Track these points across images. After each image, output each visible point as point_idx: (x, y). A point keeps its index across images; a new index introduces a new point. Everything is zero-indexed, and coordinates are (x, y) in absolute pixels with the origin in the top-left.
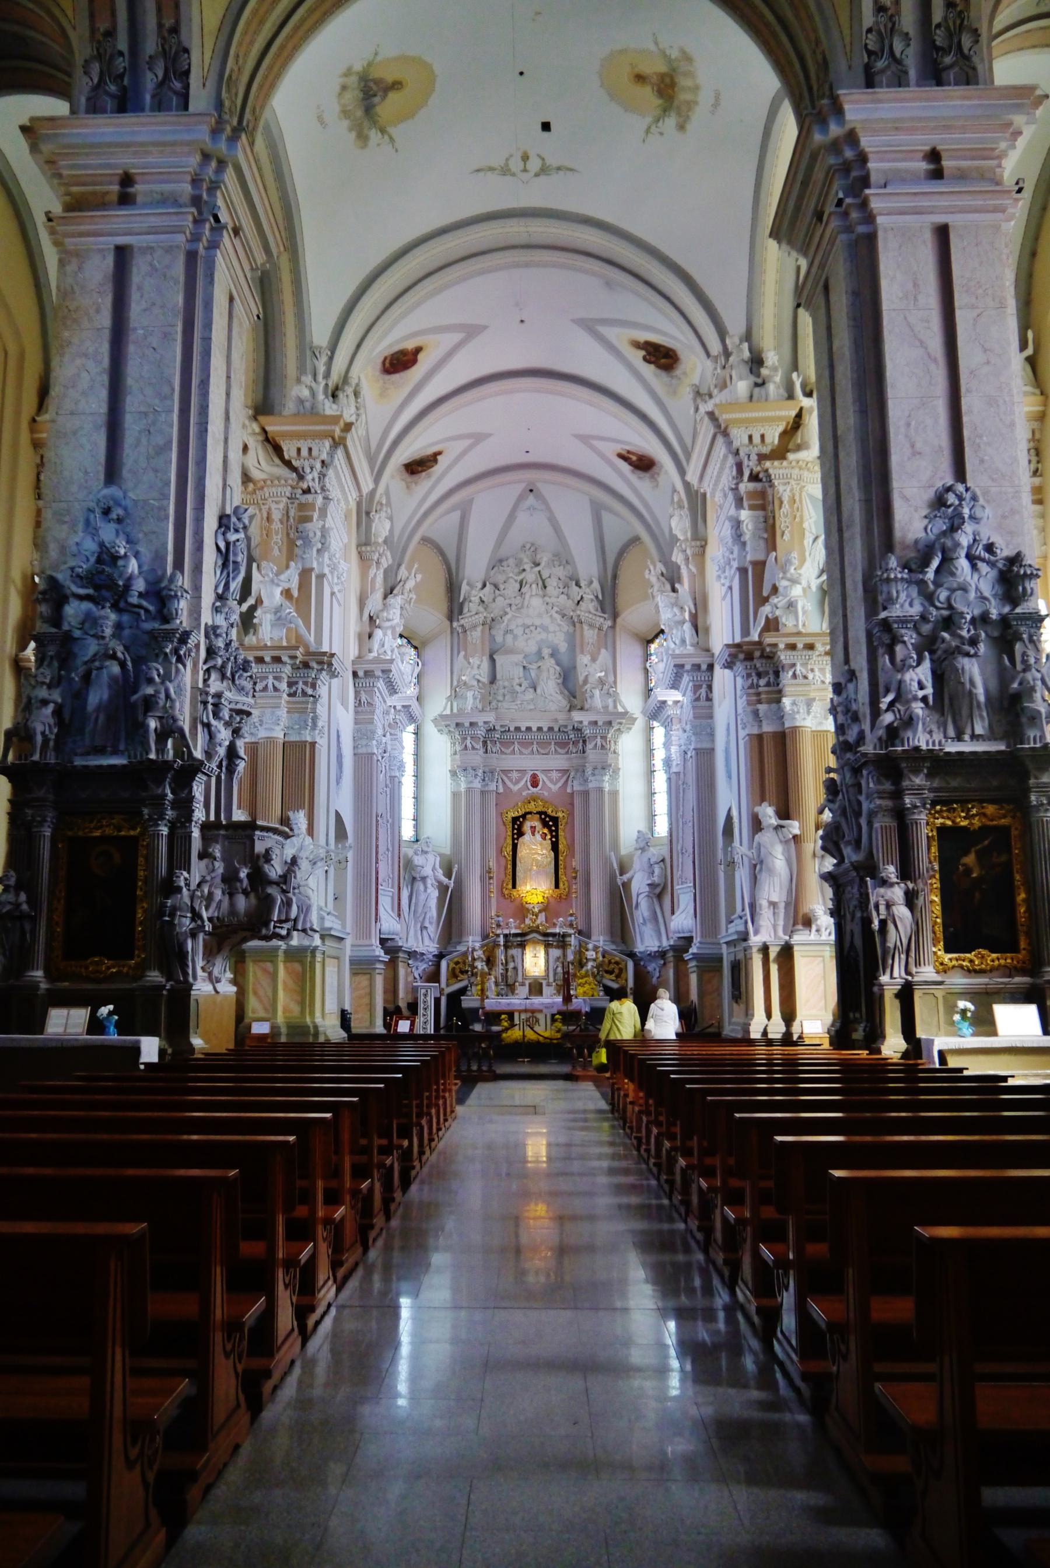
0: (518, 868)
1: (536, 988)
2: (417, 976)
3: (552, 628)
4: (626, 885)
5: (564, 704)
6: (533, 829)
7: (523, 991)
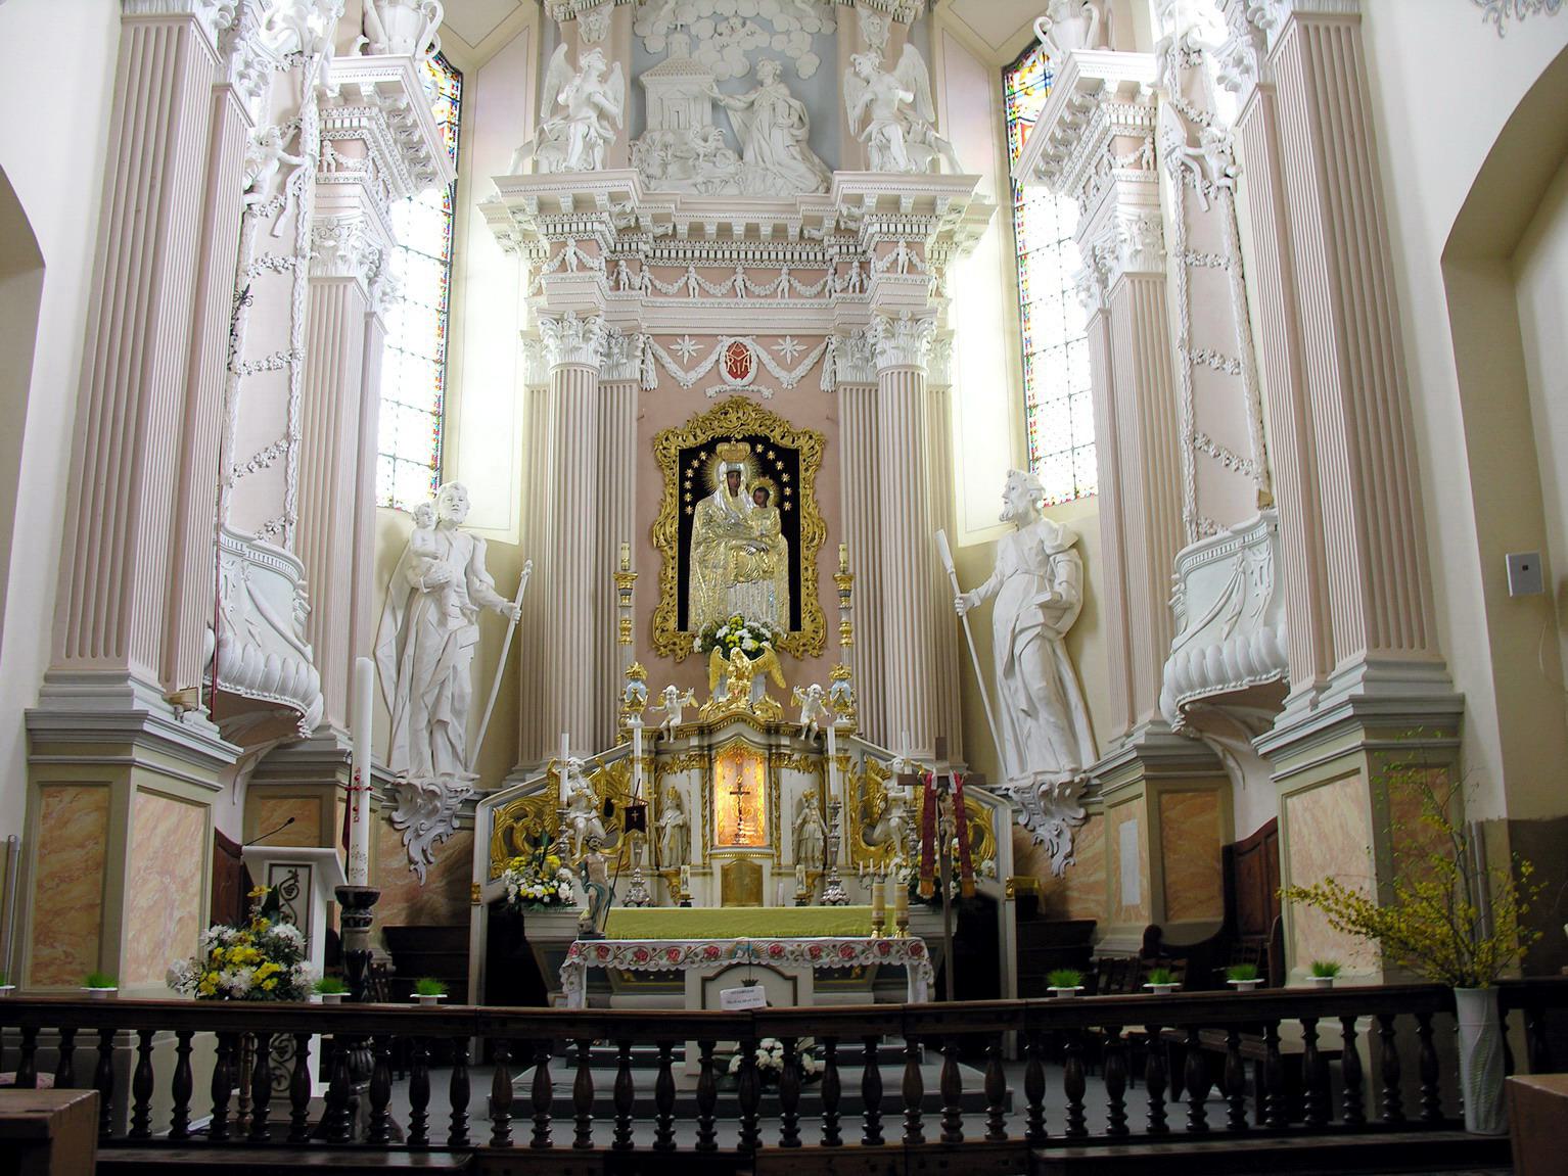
0: (692, 584)
1: (743, 883)
2: (418, 857)
3: (780, 24)
4: (981, 616)
5: (812, 181)
6: (735, 476)
7: (705, 894)
